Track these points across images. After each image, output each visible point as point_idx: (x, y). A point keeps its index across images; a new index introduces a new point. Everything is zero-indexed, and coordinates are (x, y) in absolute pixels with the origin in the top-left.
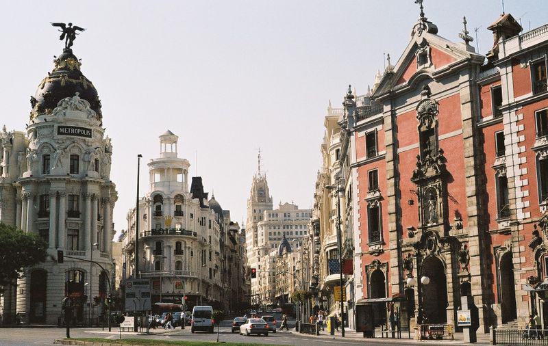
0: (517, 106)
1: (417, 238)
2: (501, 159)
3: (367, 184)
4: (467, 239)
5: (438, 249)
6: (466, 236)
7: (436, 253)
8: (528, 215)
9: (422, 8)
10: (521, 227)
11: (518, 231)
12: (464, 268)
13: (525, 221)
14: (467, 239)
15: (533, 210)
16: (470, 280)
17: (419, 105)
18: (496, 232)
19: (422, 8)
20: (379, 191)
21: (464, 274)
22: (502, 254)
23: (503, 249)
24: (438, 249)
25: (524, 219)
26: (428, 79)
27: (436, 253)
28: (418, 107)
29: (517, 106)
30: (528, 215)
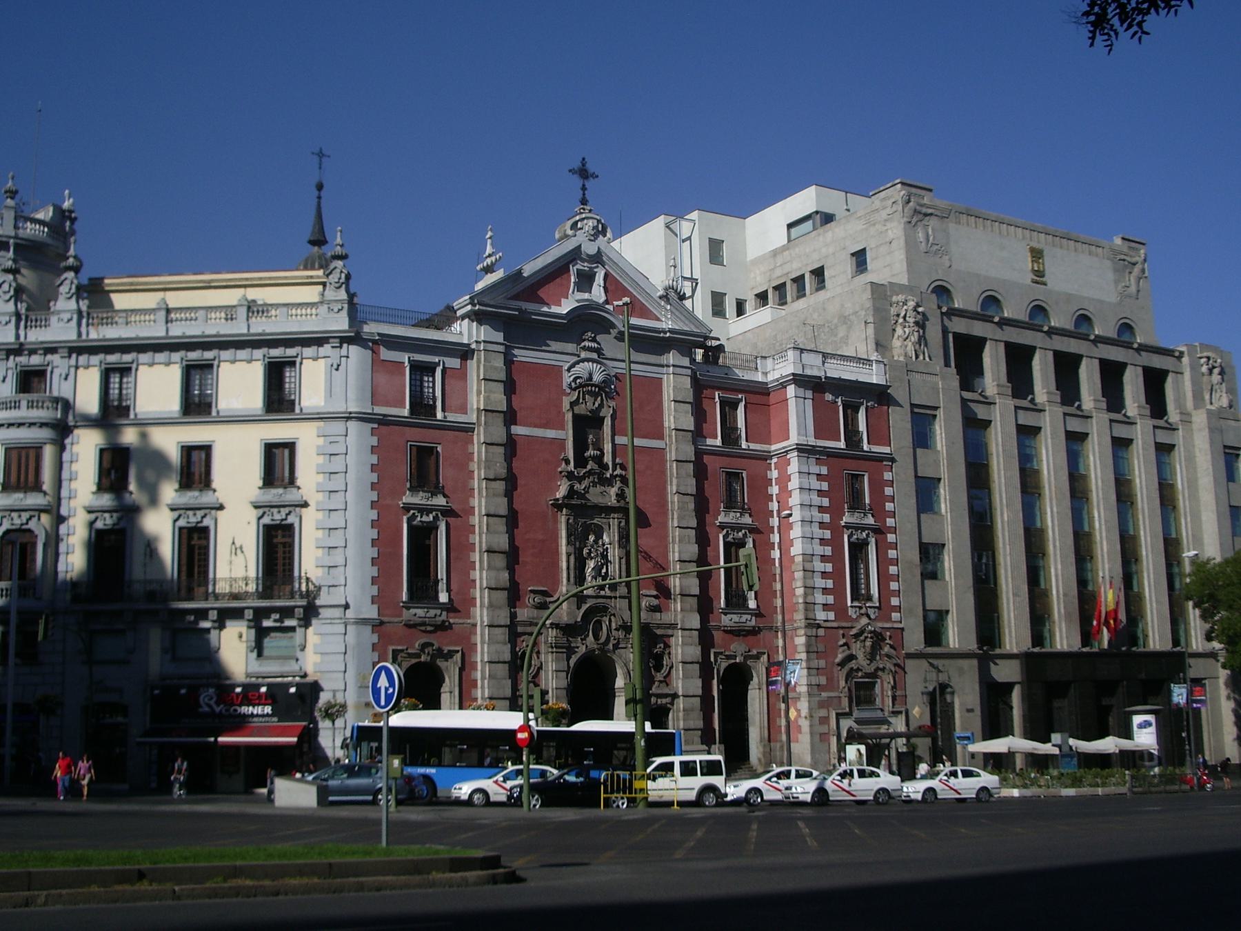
0: (820, 453)
1: (565, 613)
2: (732, 514)
3: (404, 469)
4: (670, 632)
5: (612, 642)
6: (673, 626)
7: (611, 646)
8: (831, 616)
9: (584, 188)
10: (821, 632)
11: (817, 636)
12: (661, 682)
13: (829, 625)
14: (670, 632)
15: (839, 608)
16: (672, 704)
17: (578, 363)
18: (718, 628)
19: (584, 188)
20: (445, 496)
21: (659, 691)
22: (724, 665)
23: (728, 657)
24: (612, 642)
25: (825, 621)
26: (604, 326)
27: (611, 646)
28: (573, 366)
29: (820, 453)
30: (831, 616)
